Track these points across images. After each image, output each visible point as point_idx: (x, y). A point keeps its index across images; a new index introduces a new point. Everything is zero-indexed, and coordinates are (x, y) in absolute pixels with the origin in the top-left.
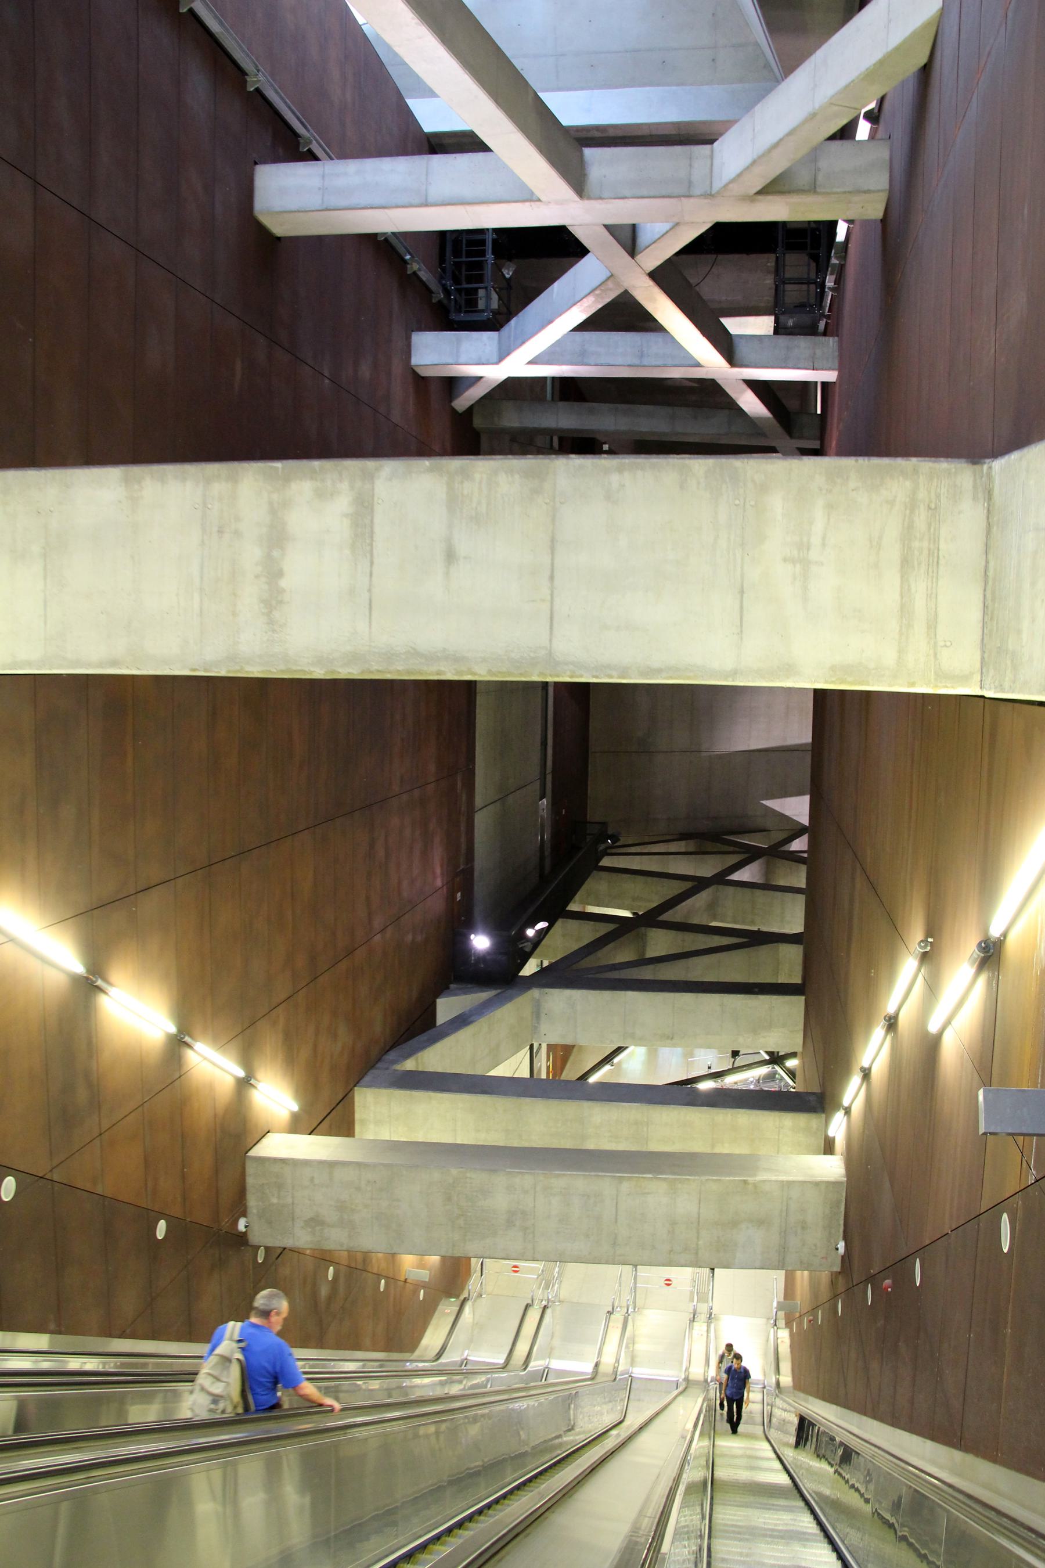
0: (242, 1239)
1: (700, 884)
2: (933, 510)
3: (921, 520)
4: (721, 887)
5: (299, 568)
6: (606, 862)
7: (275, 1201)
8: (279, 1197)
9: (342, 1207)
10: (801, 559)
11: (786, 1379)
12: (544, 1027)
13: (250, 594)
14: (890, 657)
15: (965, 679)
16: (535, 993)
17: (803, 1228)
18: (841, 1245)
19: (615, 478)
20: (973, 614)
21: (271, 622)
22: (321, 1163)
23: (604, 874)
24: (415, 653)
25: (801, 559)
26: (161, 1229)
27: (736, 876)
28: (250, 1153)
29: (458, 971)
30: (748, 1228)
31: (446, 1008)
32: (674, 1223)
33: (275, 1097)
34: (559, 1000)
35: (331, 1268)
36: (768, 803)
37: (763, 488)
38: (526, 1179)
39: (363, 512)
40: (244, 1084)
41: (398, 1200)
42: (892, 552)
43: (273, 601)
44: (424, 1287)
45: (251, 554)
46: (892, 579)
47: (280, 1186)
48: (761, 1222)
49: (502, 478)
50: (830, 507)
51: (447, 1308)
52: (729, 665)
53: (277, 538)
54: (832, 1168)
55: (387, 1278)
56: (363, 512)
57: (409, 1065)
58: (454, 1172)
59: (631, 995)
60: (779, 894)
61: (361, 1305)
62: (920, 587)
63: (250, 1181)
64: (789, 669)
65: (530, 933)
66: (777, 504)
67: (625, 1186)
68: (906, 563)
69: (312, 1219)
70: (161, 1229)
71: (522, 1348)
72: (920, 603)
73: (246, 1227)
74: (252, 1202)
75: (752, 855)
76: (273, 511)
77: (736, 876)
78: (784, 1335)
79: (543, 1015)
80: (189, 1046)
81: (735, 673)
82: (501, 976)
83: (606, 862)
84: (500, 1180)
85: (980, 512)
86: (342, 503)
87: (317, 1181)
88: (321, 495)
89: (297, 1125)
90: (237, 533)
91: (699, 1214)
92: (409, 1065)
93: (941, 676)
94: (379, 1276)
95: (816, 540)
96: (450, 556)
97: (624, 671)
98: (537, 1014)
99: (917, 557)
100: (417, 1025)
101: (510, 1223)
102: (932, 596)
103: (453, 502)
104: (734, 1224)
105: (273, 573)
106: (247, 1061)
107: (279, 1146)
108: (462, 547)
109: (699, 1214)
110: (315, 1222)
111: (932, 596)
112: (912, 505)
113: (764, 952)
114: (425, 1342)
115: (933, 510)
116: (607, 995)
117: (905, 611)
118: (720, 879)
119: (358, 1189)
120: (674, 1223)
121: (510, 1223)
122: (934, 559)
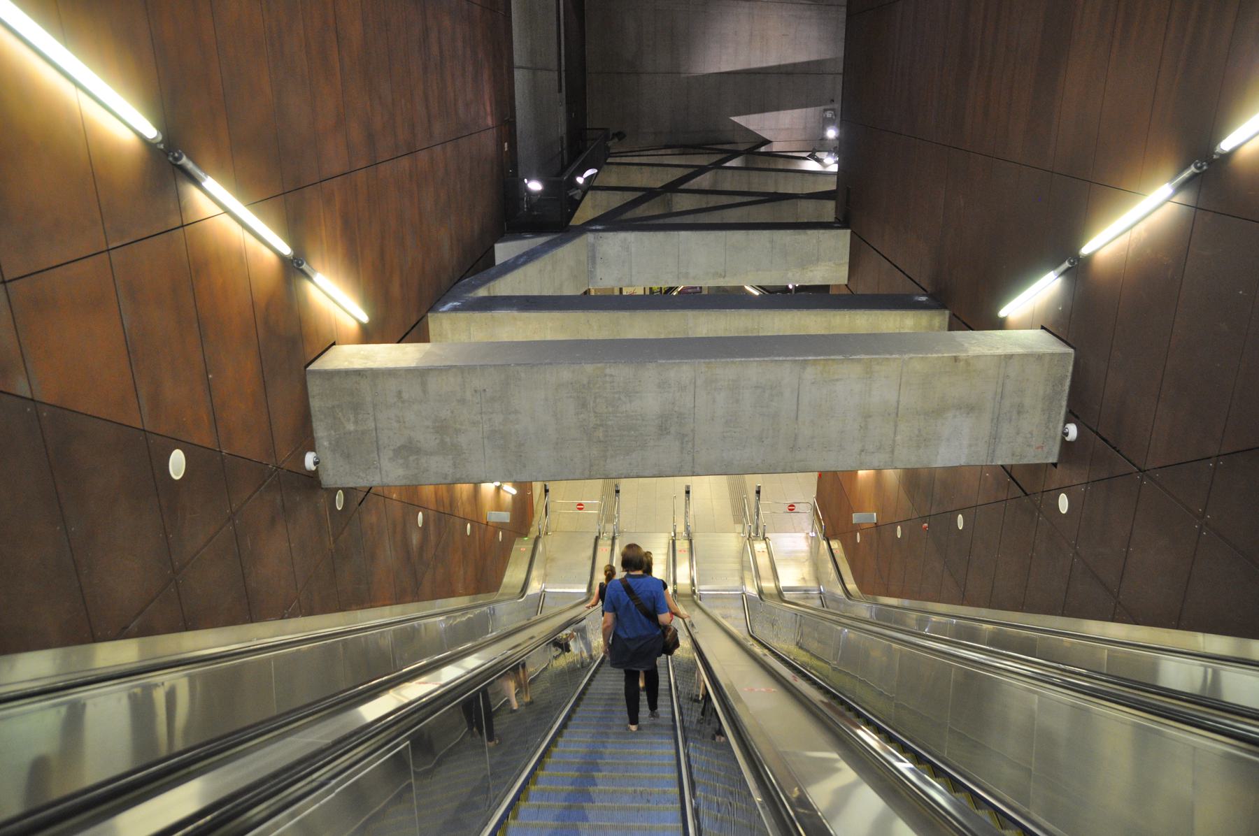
0: (312, 480)
1: (701, 170)
4: (720, 171)
6: (609, 160)
7: (351, 427)
8: (356, 422)
9: (441, 428)
11: (852, 586)
12: (600, 271)
16: (590, 237)
17: (1019, 413)
18: (1073, 431)
22: (409, 371)
23: (614, 168)
26: (177, 463)
27: (728, 164)
28: (311, 367)
29: (515, 217)
30: (955, 416)
31: (504, 251)
32: (867, 416)
33: (334, 298)
34: (614, 244)
35: (420, 514)
36: (735, 119)
38: (684, 371)
40: (293, 268)
41: (516, 412)
44: (502, 529)
47: (356, 407)
48: (970, 409)
51: (522, 548)
55: (472, 521)
57: (482, 292)
58: (589, 368)
59: (683, 233)
60: (773, 173)
63: (315, 404)
65: (580, 180)
67: (810, 373)
69: (403, 447)
70: (177, 463)
73: (316, 463)
74: (321, 431)
75: (734, 154)
77: (728, 164)
78: (835, 545)
79: (598, 261)
80: (196, 182)
82: (554, 221)
83: (609, 160)
84: (650, 374)
87: (405, 396)
89: (368, 335)
91: (898, 402)
94: (465, 520)
98: (593, 259)
100: (479, 263)
101: (663, 430)
104: (939, 412)
106: (293, 226)
107: (350, 356)
109: (898, 402)
110: (408, 450)
113: (785, 205)
114: (506, 580)
116: (660, 235)
118: (718, 165)
119: (462, 401)
120: (867, 416)
121: (663, 430)
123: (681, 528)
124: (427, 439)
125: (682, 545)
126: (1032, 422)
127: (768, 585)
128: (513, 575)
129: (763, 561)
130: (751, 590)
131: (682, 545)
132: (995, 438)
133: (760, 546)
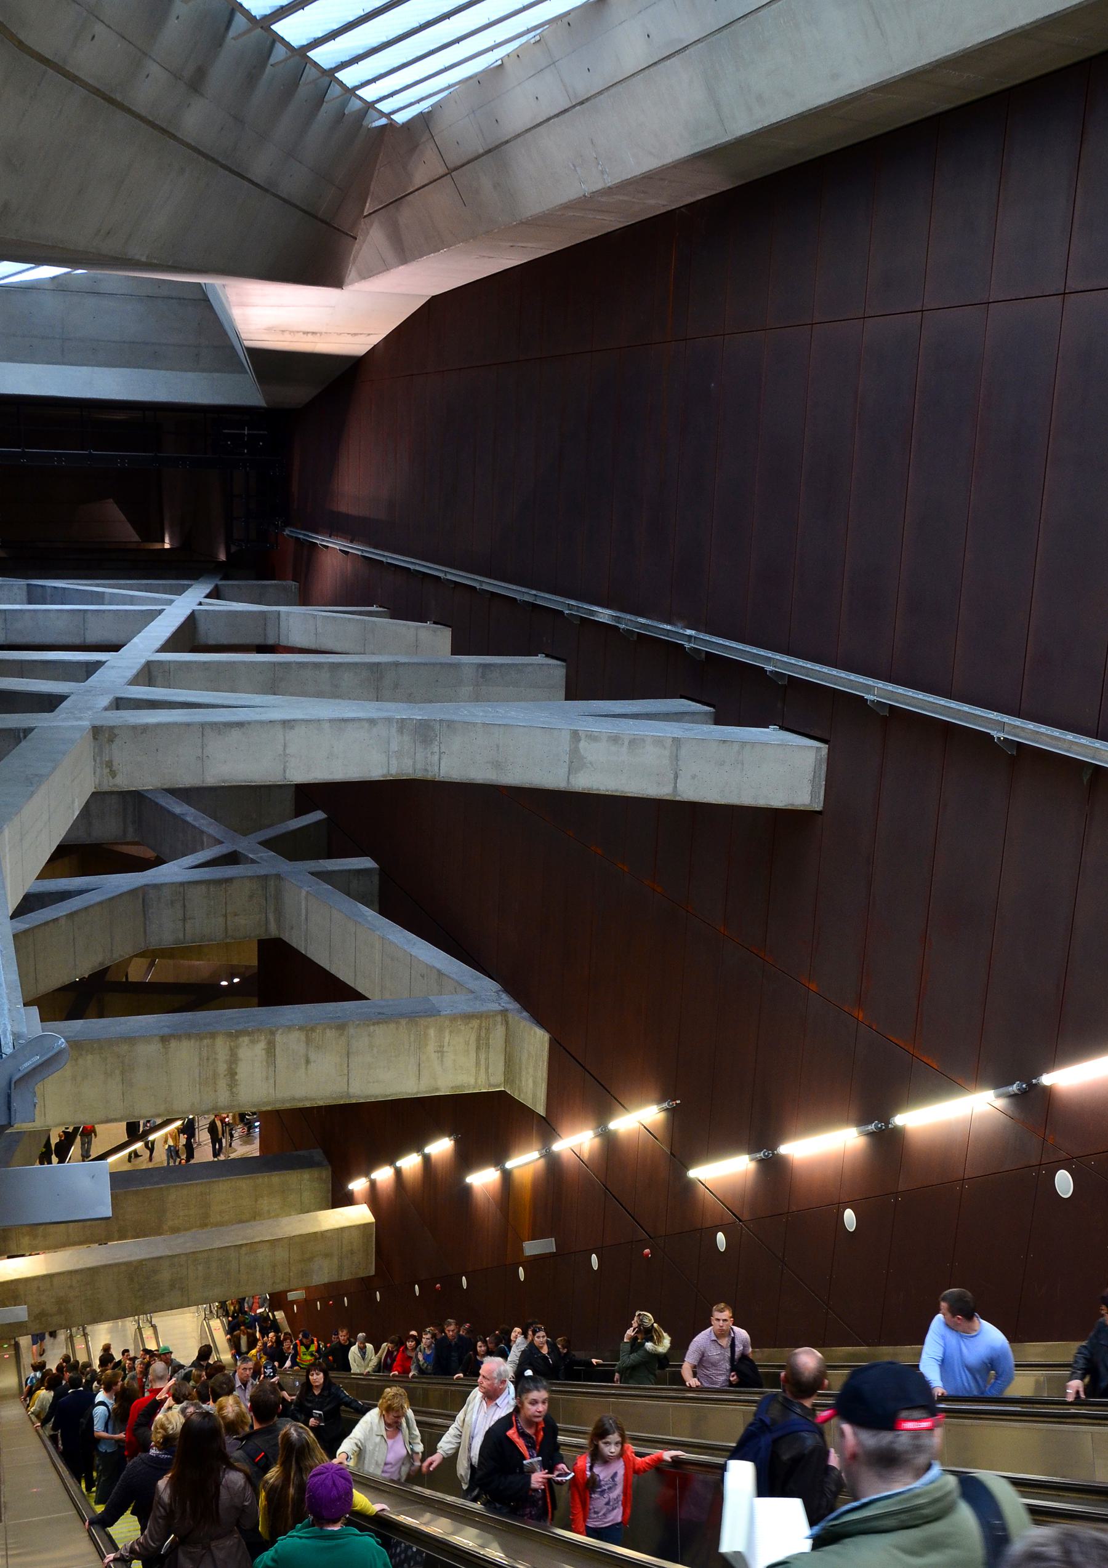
2: (488, 1029)
3: (483, 1034)
5: (243, 1070)
10: (441, 1052)
13: (222, 1084)
14: (472, 1081)
15: (499, 1086)
19: (372, 1028)
20: (501, 1064)
21: (232, 1093)
24: (294, 1099)
25: (441, 1052)
32: (274, 1266)
37: (427, 1027)
45: (222, 1068)
46: (473, 1054)
48: (327, 1255)
49: (328, 1031)
50: (451, 1032)
52: (415, 1091)
62: (483, 1057)
64: (437, 1089)
66: (432, 1032)
68: (478, 1048)
72: (483, 1061)
76: (231, 1049)
81: (417, 1093)
85: (504, 1028)
88: (253, 1042)
90: (216, 1059)
93: (490, 1085)
95: (446, 1044)
96: (308, 1062)
97: (377, 1097)
99: (482, 1044)
102: (487, 1059)
103: (308, 1041)
104: (311, 1259)
105: (232, 1074)
108: (312, 1057)
111: (487, 1059)
112: (480, 1027)
115: (488, 1029)
117: (478, 1064)
121: (172, 1286)
122: (488, 1045)
132: (340, 1268)
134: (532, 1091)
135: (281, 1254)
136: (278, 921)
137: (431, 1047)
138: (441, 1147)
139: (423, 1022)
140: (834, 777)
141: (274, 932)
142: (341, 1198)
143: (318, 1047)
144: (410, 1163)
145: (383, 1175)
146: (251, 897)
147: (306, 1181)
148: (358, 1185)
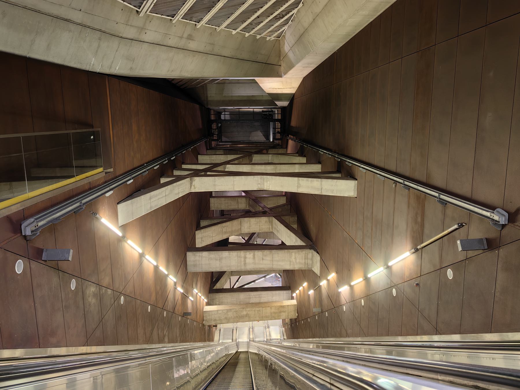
5: (248, 261)
10: (295, 259)
11: (285, 337)
13: (243, 263)
39: (254, 255)
42: (304, 258)
43: (245, 264)
45: (243, 259)
53: (245, 258)
54: (294, 302)
56: (254, 255)
61: (205, 332)
66: (293, 254)
68: (305, 259)
71: (234, 338)
74: (205, 318)
78: (283, 329)
86: (252, 254)
92: (215, 288)
101: (246, 316)
110: (215, 320)
117: (305, 263)
123: (251, 326)
124: (217, 319)
125: (251, 330)
126: (293, 313)
127: (268, 338)
128: (216, 338)
129: (268, 334)
130: (265, 340)
131: (251, 330)
132: (288, 315)
133: (267, 329)
134: (317, 269)
135: (273, 310)
136: (272, 228)
137: (293, 257)
138: (305, 284)
139: (291, 251)
140: (360, 190)
141: (271, 230)
142: (292, 298)
143: (265, 256)
144: (301, 288)
145: (298, 292)
146: (266, 222)
147: (284, 294)
148: (294, 295)
